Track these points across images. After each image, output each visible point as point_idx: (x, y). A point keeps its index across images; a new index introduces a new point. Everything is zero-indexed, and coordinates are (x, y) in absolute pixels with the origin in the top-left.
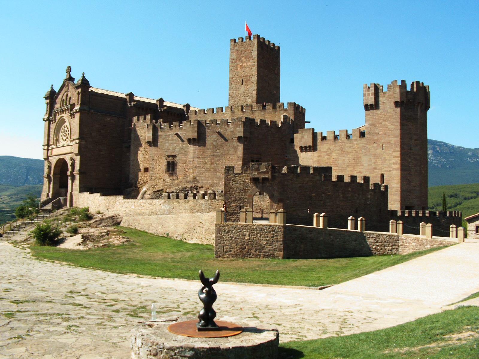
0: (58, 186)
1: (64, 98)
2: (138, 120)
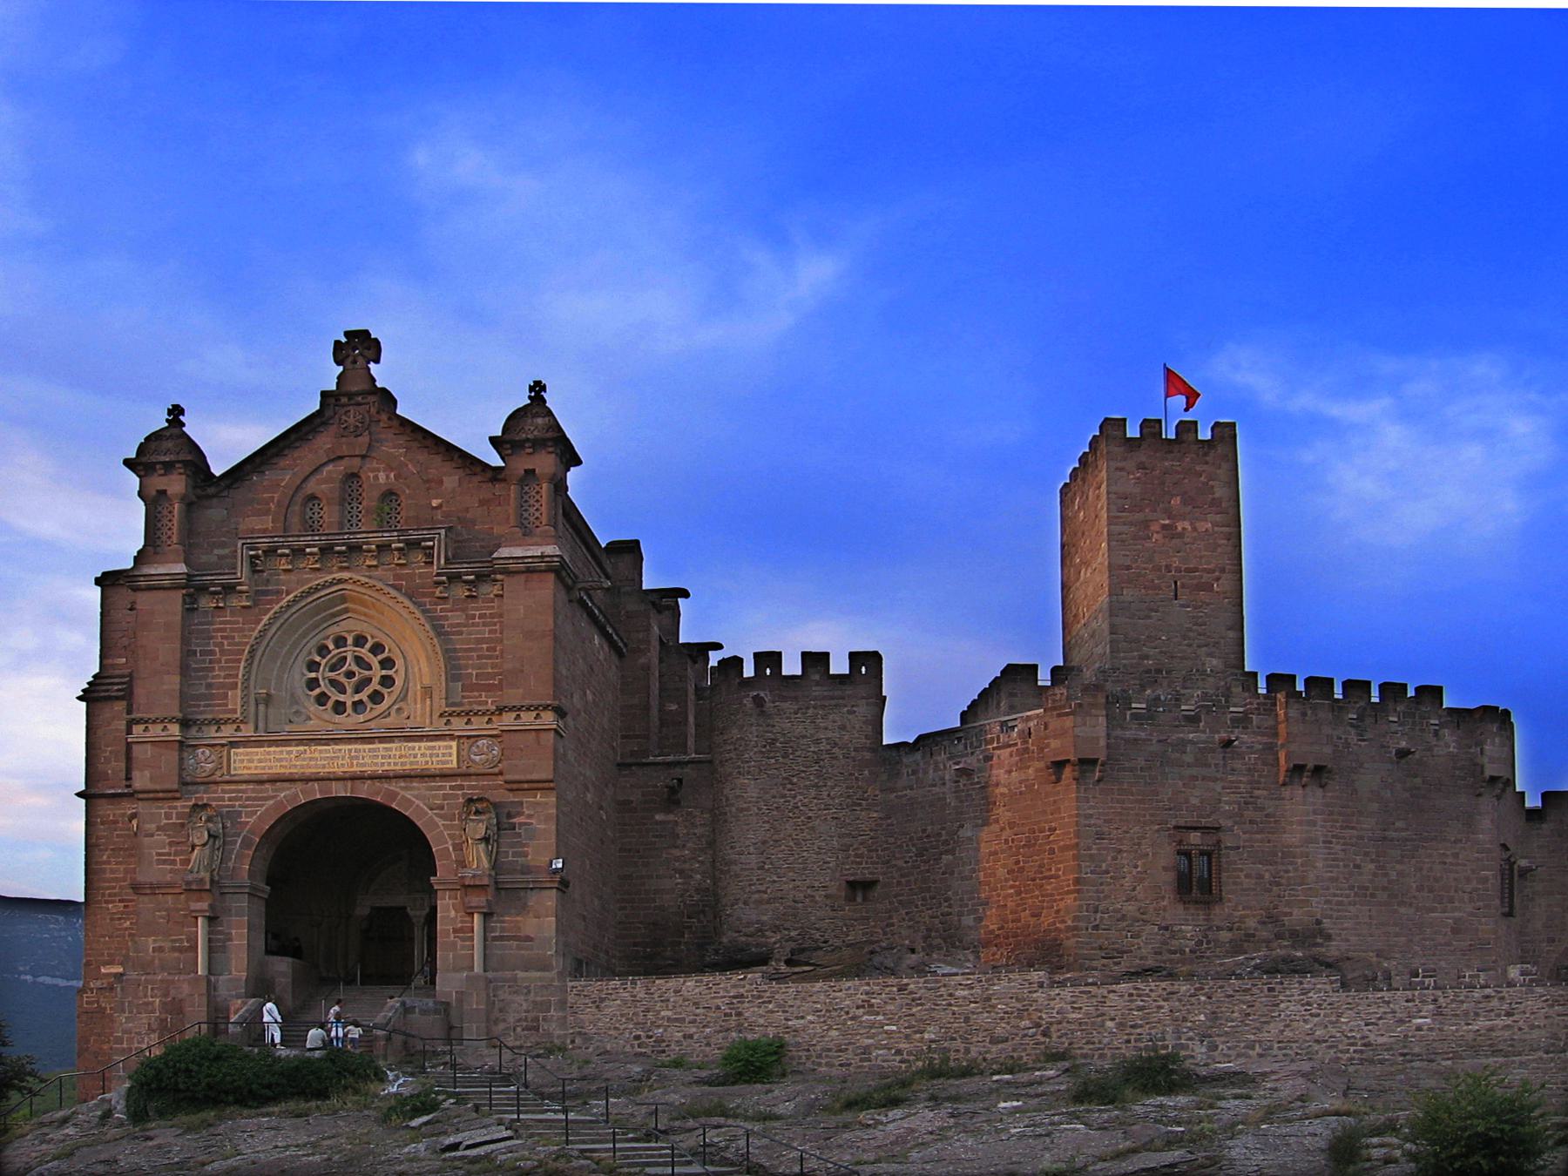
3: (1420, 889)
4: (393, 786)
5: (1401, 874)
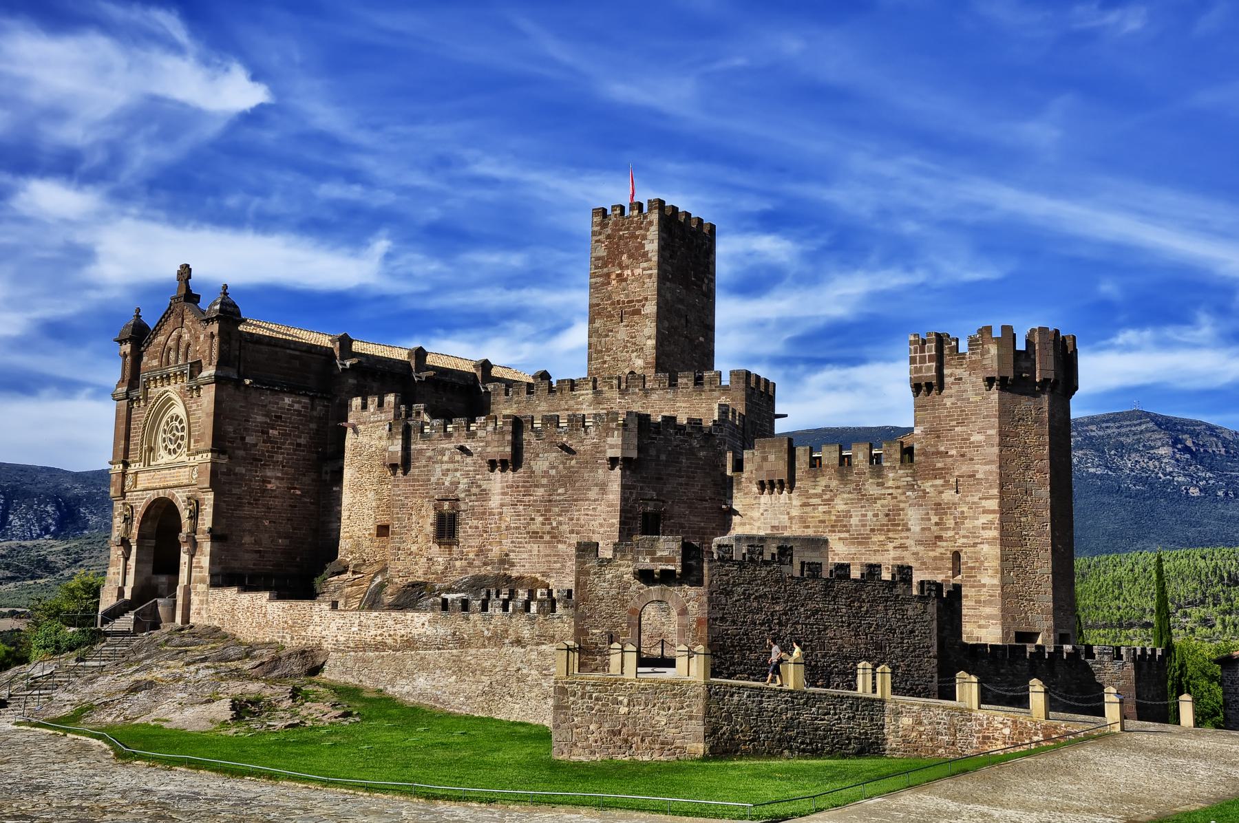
0: (149, 569)
1: (171, 343)
2: (364, 407)
3: (572, 532)
4: (174, 491)
5: (560, 523)
